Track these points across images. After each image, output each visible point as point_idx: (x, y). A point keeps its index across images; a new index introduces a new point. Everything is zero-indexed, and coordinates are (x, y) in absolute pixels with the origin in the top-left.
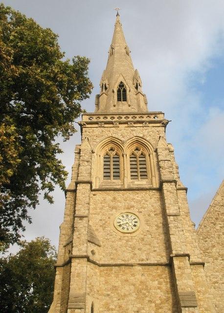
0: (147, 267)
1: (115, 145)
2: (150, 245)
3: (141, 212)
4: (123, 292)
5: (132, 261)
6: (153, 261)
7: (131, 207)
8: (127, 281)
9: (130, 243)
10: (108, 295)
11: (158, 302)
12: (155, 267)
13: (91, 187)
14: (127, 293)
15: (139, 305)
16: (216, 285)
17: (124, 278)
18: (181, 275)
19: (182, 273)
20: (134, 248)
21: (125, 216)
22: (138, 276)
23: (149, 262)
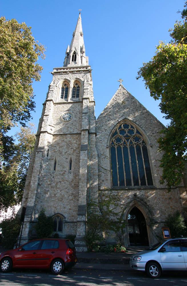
1: (66, 83)
2: (75, 126)
3: (73, 112)
4: (61, 145)
6: (75, 132)
7: (70, 110)
9: (67, 125)
10: (55, 146)
12: (76, 135)
13: (53, 102)
14: (63, 145)
15: (67, 150)
16: (101, 141)
17: (62, 139)
18: (83, 138)
19: (84, 137)
20: (68, 127)
21: (66, 114)
22: (68, 139)
23: (74, 133)
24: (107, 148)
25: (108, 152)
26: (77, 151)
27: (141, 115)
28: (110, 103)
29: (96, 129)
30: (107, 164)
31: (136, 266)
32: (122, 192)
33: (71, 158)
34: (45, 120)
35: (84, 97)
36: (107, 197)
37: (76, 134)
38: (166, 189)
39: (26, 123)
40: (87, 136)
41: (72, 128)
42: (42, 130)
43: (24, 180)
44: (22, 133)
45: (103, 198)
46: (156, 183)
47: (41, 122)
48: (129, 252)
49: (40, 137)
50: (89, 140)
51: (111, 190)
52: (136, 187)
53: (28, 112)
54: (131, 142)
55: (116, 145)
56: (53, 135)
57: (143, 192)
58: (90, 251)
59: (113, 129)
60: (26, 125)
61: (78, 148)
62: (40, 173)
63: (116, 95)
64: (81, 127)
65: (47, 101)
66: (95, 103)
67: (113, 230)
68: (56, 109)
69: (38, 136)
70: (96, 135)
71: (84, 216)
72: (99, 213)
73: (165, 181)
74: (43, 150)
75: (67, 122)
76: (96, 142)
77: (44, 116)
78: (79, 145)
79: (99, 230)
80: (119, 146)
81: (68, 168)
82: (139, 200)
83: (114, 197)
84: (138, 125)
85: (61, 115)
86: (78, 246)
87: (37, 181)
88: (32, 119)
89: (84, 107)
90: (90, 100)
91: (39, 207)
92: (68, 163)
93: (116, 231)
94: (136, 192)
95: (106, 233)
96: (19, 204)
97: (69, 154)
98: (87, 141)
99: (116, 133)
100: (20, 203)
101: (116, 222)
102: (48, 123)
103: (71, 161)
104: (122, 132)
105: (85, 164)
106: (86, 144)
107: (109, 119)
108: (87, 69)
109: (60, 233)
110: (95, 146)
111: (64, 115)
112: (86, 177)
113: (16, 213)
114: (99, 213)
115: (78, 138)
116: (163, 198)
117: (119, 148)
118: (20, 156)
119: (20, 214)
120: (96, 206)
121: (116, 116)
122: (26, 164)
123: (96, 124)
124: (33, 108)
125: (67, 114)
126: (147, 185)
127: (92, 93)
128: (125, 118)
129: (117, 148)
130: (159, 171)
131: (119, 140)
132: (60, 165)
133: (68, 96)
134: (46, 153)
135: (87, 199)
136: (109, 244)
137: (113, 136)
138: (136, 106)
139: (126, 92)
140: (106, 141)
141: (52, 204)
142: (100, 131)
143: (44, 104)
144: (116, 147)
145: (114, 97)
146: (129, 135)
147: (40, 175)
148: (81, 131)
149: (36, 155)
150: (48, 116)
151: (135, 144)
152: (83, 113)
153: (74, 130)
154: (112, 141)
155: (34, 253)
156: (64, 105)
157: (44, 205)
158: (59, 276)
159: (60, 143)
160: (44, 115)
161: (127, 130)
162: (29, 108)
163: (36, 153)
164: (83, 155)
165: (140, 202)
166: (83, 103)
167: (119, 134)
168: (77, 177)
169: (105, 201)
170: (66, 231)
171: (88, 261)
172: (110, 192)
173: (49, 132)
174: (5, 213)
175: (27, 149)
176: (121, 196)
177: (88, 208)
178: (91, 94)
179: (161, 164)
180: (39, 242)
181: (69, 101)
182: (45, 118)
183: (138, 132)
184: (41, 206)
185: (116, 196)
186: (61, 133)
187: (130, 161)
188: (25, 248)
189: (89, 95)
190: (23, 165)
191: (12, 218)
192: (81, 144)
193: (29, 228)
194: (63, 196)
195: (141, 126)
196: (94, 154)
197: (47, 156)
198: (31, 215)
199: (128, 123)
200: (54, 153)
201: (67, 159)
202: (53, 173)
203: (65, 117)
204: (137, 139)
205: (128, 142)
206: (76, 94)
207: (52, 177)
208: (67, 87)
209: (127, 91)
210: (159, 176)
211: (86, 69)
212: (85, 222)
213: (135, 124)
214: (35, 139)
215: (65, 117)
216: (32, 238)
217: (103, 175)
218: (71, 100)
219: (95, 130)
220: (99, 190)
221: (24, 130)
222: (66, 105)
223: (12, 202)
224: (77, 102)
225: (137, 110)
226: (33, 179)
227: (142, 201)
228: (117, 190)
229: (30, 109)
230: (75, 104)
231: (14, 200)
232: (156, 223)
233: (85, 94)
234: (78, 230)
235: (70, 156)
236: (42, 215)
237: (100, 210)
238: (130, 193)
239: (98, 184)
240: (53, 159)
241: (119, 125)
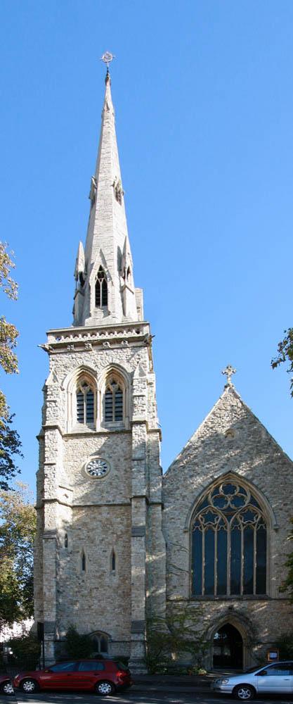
0: (112, 507)
1: (86, 377)
2: (117, 488)
3: (111, 457)
4: (91, 527)
5: (99, 503)
6: (118, 502)
8: (95, 518)
9: (99, 487)
10: (80, 529)
11: (119, 533)
12: (120, 507)
13: (61, 433)
15: (104, 536)
17: (93, 516)
22: (105, 515)
24: (185, 532)
25: (186, 541)
26: (125, 537)
27: (266, 464)
28: (197, 433)
29: (163, 495)
30: (183, 560)
31: (220, 689)
32: (209, 603)
33: (113, 549)
34: (49, 476)
35: (135, 418)
36: (180, 610)
37: (119, 505)
38: (288, 599)
39: (8, 482)
40: (144, 509)
41: (111, 492)
42: (47, 496)
43: (30, 583)
44: (6, 504)
45: (175, 611)
46: (272, 591)
47: (40, 479)
48: (211, 675)
49: (45, 510)
50: (148, 517)
51: (188, 601)
52: (235, 596)
53: (6, 456)
54: (236, 522)
55: (205, 527)
56: (73, 507)
57: (245, 604)
58: (152, 673)
59: (199, 495)
60: (9, 486)
61: (127, 532)
62: (57, 574)
63: (214, 414)
64: (131, 491)
65: (45, 429)
66: (160, 434)
67: (189, 651)
68: (70, 448)
69: (40, 508)
70: (163, 508)
71: (141, 635)
72: (166, 631)
73: (289, 587)
74: (55, 536)
75: (99, 480)
76: (163, 521)
77: (46, 467)
78: (128, 526)
79: (166, 652)
80: (210, 528)
81: (108, 567)
82: (236, 614)
83: (193, 610)
84: (256, 487)
85: (83, 464)
86: (134, 668)
87: (55, 587)
88: (19, 472)
89: (134, 446)
90: (150, 428)
91: (64, 622)
92: (109, 558)
93: (193, 653)
94: (232, 604)
95: (177, 655)
96: (30, 618)
97: (110, 544)
98: (144, 519)
99: (206, 503)
100: (32, 617)
101: (194, 642)
102: (57, 482)
103: (113, 555)
104: (219, 501)
105: (142, 561)
106: (141, 524)
107: (192, 473)
108: (140, 335)
109: (104, 654)
110: (160, 528)
111: (91, 464)
112: (143, 580)
113: (28, 629)
114: (166, 631)
115: (126, 514)
116: (278, 613)
117: (210, 533)
118: (12, 547)
119: (36, 630)
120: (162, 622)
121: (208, 466)
122: (28, 560)
123: (163, 484)
124: (17, 448)
125: (97, 462)
126: (255, 593)
127: (155, 407)
128: (230, 471)
129: (206, 532)
130: (281, 572)
131: (210, 517)
132: (92, 562)
133: (95, 417)
134: (62, 541)
135: (146, 613)
136: (180, 666)
137: (200, 507)
138: (259, 442)
139: (240, 405)
140: (183, 519)
141: (87, 619)
142: (172, 500)
143: (41, 438)
144: (203, 531)
145: (207, 418)
146: (233, 507)
147: (58, 578)
148: (131, 499)
149: (44, 545)
150: (54, 466)
151: (244, 525)
152: (134, 460)
153: (114, 496)
154: (197, 520)
155: (69, 675)
156: (88, 439)
157: (72, 620)
158: (108, 697)
159: (88, 523)
160: (46, 463)
161: (229, 498)
162: (7, 448)
163: (43, 541)
164: (137, 546)
165: (238, 617)
166: (133, 434)
167: (213, 506)
168: (127, 581)
169: (176, 615)
170: (113, 651)
171: (150, 684)
172: (187, 604)
173: (61, 501)
174: (10, 630)
175: (23, 534)
176: (206, 610)
177: (148, 624)
178: (151, 410)
179: (289, 561)
180: (72, 664)
181: (99, 429)
182: (47, 470)
183: (253, 501)
184: (69, 622)
185: (198, 608)
186: (88, 504)
187: (229, 556)
188: (54, 669)
189: (146, 413)
190: (22, 562)
191: (24, 636)
192: (131, 524)
193: (55, 648)
194: (105, 608)
195: (263, 490)
196: (157, 543)
197: (66, 546)
198: (55, 632)
199: (234, 481)
200: (79, 542)
201: (104, 551)
202: (81, 574)
203: (92, 468)
204: (249, 515)
205: (229, 521)
206: (114, 410)
207: (80, 581)
208: (90, 391)
209: (241, 402)
210: (279, 580)
211: (138, 333)
212: (143, 642)
213: (249, 484)
214: (36, 514)
215: (92, 468)
216: (60, 659)
217: (175, 578)
218: (102, 425)
219: (160, 497)
220: (168, 600)
221: (7, 497)
222: (92, 439)
223: (17, 616)
224: (117, 433)
225: (259, 453)
226: (45, 583)
227: (243, 617)
228: (199, 601)
229: (10, 450)
230: (115, 437)
231: (20, 613)
232: (259, 643)
233: (135, 410)
234: (133, 650)
235: (111, 547)
236: (72, 633)
237: (169, 627)
238: (223, 606)
239: (166, 592)
240: (78, 552)
241: (213, 486)
